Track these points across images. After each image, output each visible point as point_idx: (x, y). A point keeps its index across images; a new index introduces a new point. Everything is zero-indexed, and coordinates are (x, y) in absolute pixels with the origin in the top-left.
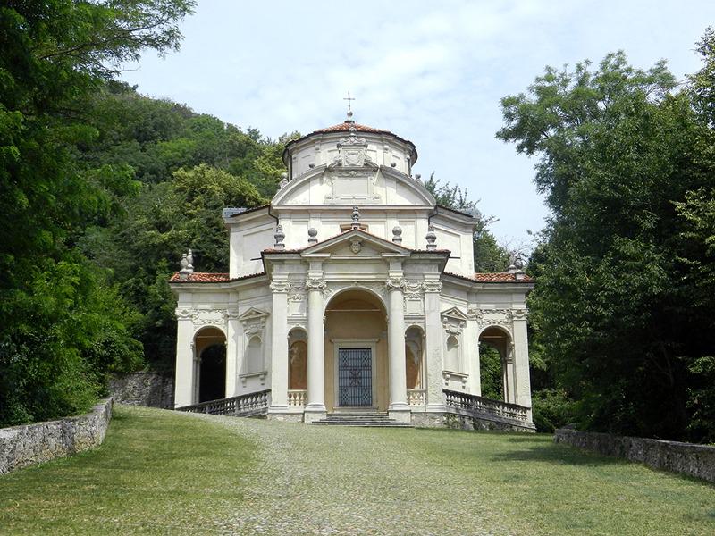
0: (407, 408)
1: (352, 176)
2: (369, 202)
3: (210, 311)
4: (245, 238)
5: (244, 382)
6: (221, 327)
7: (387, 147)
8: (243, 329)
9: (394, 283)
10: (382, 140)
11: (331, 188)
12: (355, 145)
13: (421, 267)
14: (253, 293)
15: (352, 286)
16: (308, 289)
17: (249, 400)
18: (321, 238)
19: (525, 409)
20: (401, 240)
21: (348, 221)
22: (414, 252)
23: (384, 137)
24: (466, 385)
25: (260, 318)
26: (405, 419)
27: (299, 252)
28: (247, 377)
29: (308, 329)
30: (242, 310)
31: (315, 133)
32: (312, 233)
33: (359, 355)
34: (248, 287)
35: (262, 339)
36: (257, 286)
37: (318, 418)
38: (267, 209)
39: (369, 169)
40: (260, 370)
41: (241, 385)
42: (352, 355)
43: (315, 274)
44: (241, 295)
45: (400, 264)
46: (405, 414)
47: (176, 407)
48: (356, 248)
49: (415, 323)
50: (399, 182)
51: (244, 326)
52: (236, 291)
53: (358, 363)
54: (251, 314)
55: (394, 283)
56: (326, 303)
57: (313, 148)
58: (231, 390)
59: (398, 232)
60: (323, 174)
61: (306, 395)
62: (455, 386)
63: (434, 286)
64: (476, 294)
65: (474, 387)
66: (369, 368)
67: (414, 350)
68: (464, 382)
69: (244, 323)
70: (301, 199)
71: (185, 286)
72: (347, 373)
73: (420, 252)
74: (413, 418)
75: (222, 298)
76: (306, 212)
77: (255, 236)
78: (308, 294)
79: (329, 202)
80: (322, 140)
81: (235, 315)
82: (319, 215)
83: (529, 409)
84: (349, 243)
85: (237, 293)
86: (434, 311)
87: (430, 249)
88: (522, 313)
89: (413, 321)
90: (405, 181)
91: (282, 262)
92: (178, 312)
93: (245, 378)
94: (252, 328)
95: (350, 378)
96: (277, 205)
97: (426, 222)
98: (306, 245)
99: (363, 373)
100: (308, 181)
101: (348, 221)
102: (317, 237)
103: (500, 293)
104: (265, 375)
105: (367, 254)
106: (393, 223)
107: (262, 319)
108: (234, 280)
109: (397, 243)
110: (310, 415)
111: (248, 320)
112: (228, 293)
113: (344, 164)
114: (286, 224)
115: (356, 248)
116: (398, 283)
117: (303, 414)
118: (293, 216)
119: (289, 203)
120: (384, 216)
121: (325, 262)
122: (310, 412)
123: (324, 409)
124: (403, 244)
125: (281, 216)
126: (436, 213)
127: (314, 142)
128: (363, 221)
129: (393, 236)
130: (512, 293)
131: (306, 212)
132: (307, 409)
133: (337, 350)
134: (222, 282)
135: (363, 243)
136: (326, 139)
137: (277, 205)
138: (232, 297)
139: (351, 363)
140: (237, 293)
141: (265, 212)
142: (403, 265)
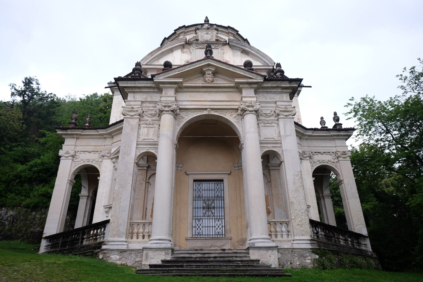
3: (90, 152)
8: (113, 165)
9: (248, 106)
10: (228, 33)
13: (272, 96)
15: (205, 113)
23: (230, 31)
31: (180, 28)
33: (212, 185)
42: (205, 186)
45: (252, 91)
46: (270, 252)
47: (44, 236)
48: (209, 77)
51: (114, 163)
53: (211, 194)
55: (248, 106)
56: (178, 129)
63: (288, 111)
64: (307, 139)
66: (222, 198)
69: (114, 160)
71: (69, 132)
72: (201, 204)
75: (100, 142)
80: (185, 33)
86: (290, 135)
88: (346, 154)
89: (268, 145)
92: (61, 153)
95: (203, 208)
96: (146, 65)
103: (325, 139)
105: (220, 82)
110: (151, 253)
113: (200, 39)
115: (209, 77)
116: (252, 106)
122: (151, 249)
123: (169, 245)
130: (334, 139)
135: (216, 73)
136: (188, 32)
137: (146, 65)
138: (108, 142)
139: (205, 194)
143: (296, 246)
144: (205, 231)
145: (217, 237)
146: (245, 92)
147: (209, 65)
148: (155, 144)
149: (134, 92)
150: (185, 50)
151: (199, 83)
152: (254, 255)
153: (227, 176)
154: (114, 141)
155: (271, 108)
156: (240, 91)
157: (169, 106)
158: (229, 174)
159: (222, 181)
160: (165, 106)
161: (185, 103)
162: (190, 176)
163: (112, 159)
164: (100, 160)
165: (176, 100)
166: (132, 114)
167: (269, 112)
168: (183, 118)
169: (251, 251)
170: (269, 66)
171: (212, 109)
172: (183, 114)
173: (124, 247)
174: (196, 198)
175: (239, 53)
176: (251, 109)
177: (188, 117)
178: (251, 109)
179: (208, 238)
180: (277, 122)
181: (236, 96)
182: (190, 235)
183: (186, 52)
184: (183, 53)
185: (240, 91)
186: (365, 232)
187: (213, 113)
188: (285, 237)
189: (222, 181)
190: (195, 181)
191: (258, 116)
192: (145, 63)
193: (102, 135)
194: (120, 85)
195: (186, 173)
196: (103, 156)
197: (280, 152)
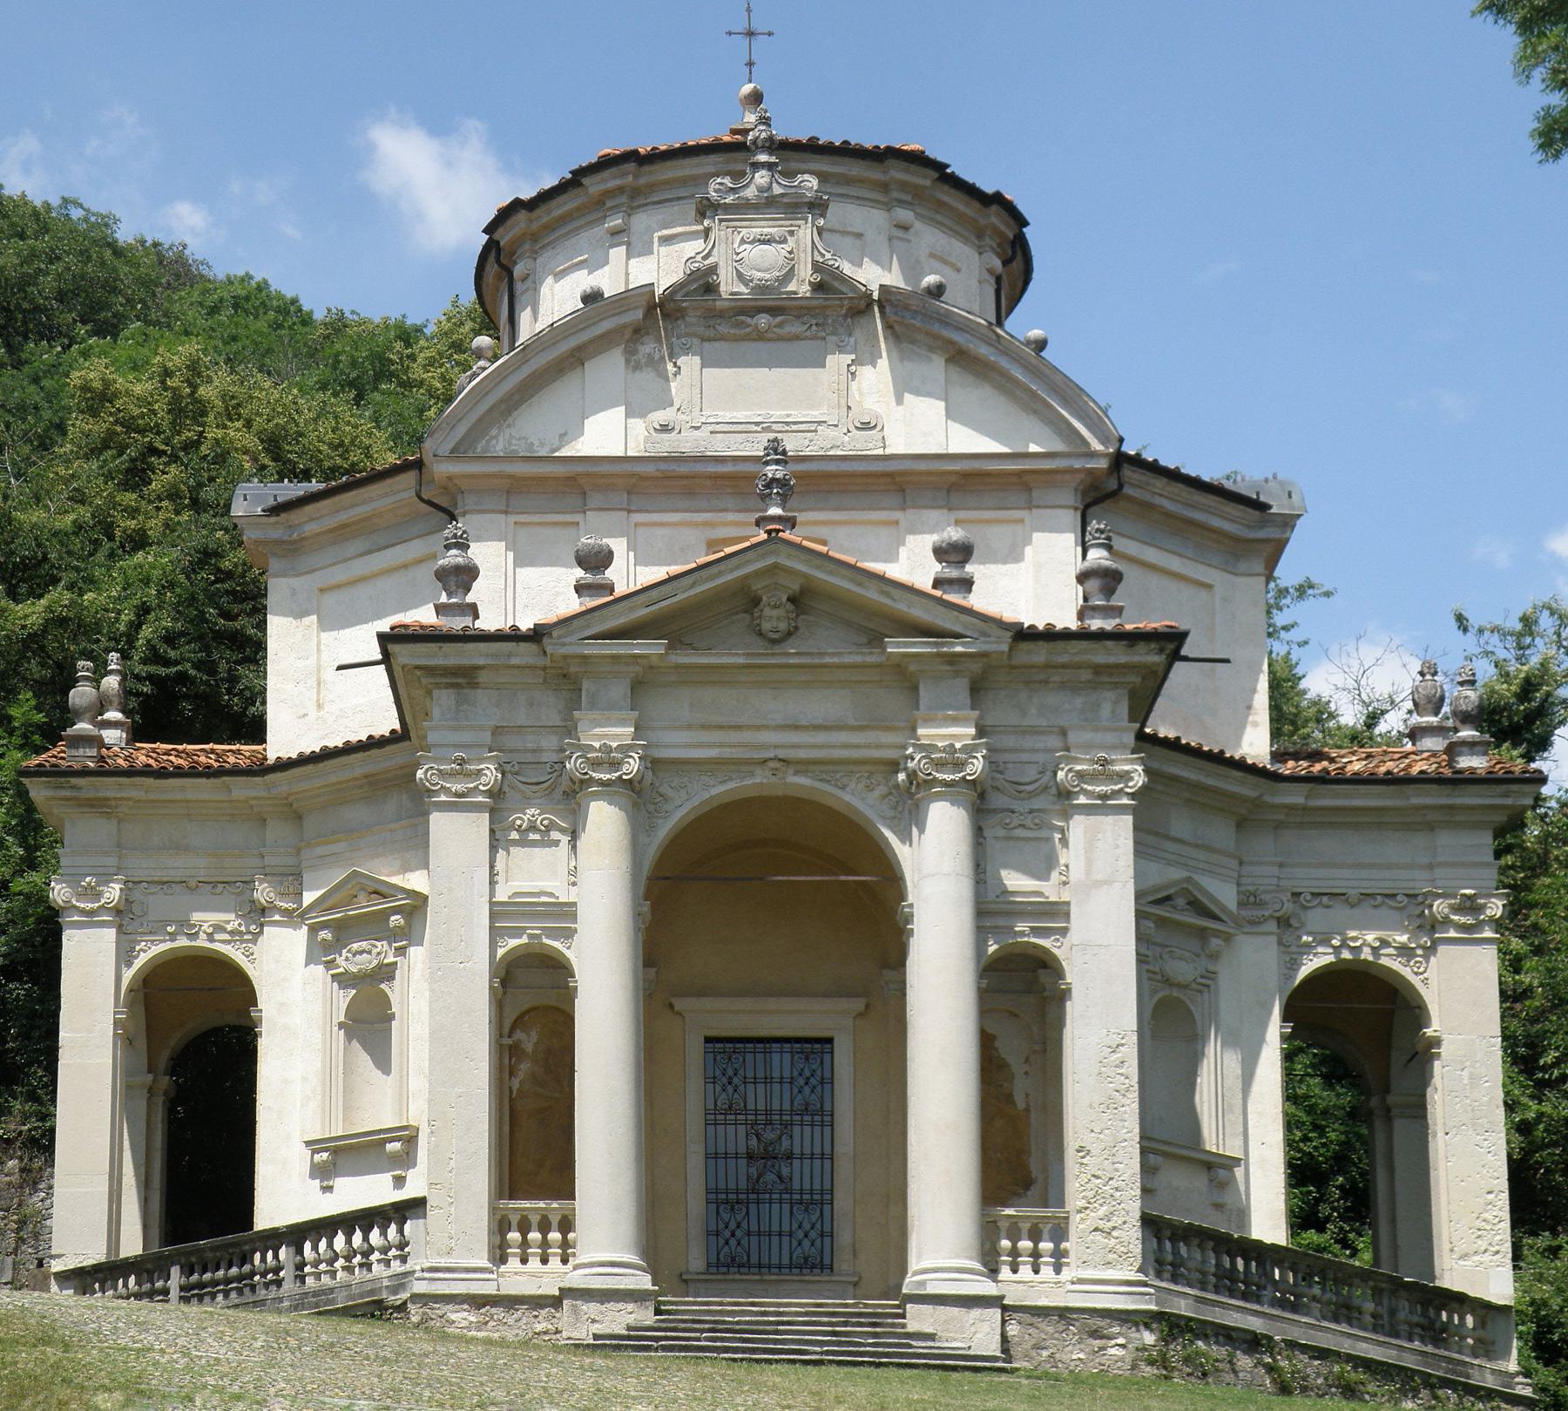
6: (235, 954)
7: (904, 214)
13: (1052, 699)
17: (339, 1241)
27: (538, 634)
28: (335, 1152)
102: (611, 574)
108: (283, 765)
113: (728, 285)
129: (935, 568)
142: (977, 690)
147: (776, 567)
167: (1031, 773)
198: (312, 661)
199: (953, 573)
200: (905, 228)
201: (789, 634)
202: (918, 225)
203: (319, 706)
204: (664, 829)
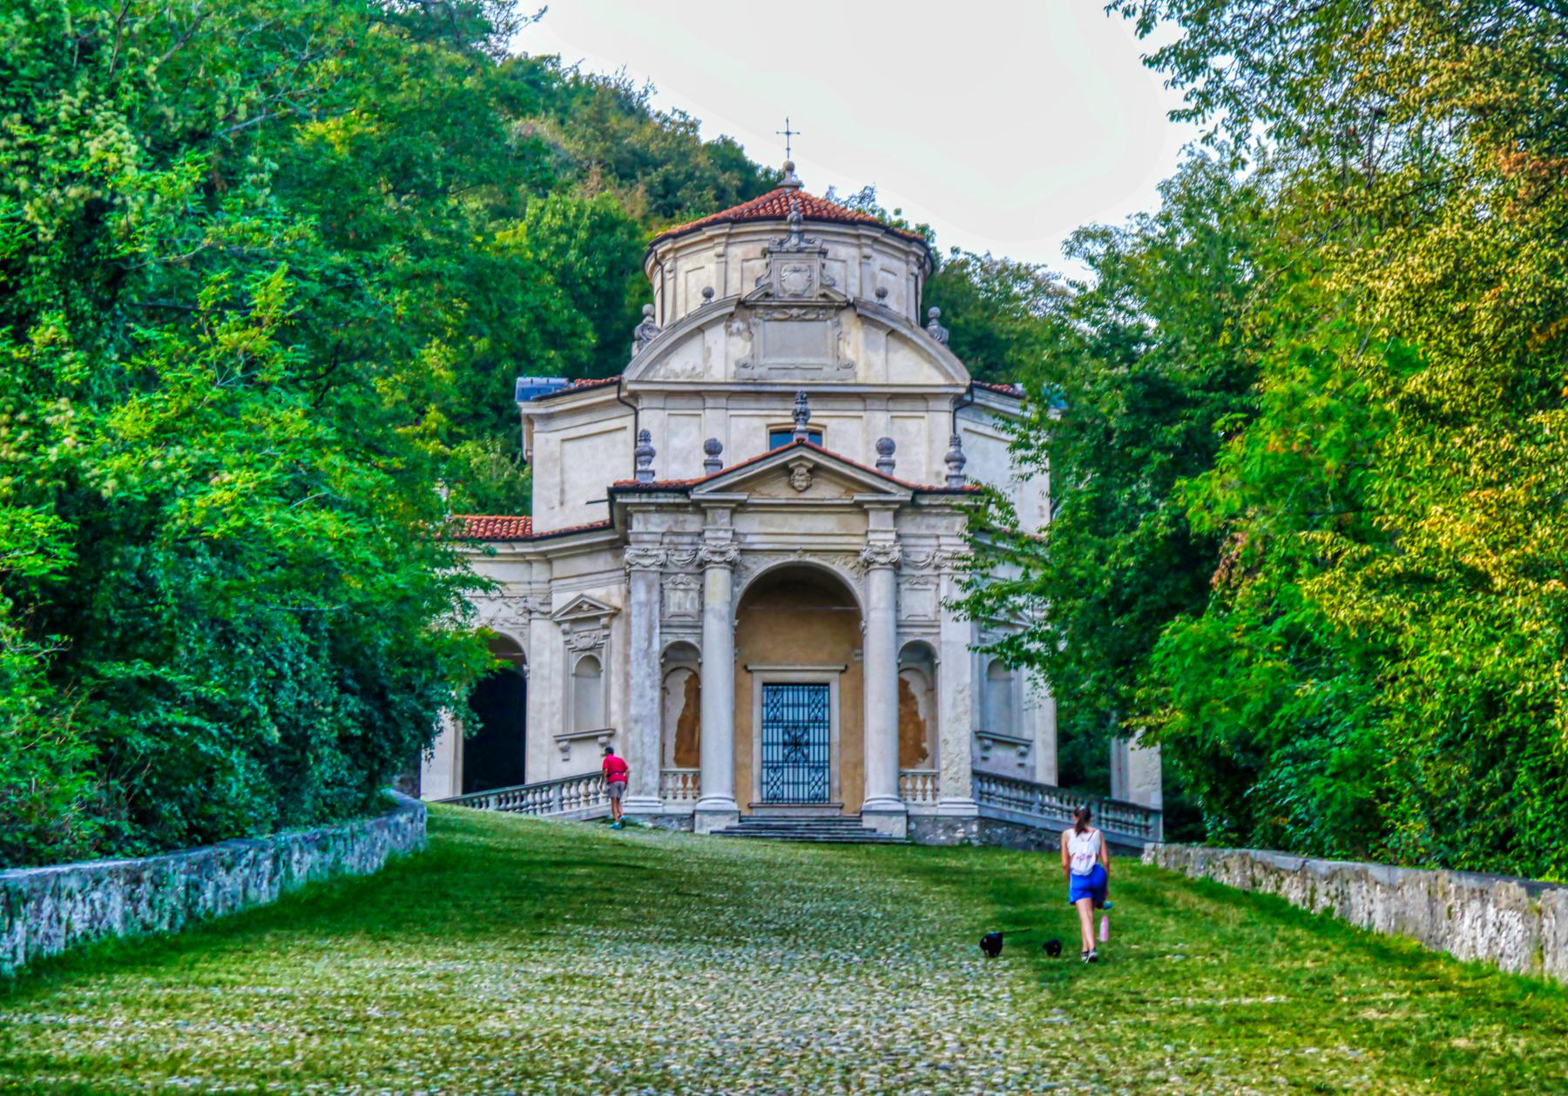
0: (901, 807)
1: (790, 319)
2: (828, 375)
4: (568, 445)
5: (564, 750)
6: (515, 636)
7: (867, 251)
8: (561, 639)
10: (858, 237)
11: (749, 345)
12: (800, 251)
13: (932, 521)
14: (583, 564)
15: (792, 558)
16: (702, 565)
17: (582, 789)
18: (728, 460)
19: (1148, 812)
20: (892, 464)
21: (782, 415)
22: (918, 492)
24: (1028, 761)
25: (597, 618)
26: (896, 828)
27: (683, 489)
28: (572, 740)
29: (701, 642)
30: (561, 600)
32: (713, 448)
33: (804, 697)
34: (574, 553)
35: (603, 666)
36: (592, 550)
37: (722, 824)
38: (615, 388)
39: (830, 306)
40: (598, 724)
41: (559, 756)
42: (788, 696)
43: (719, 533)
44: (560, 568)
45: (890, 514)
46: (894, 819)
48: (800, 482)
49: (915, 635)
50: (892, 332)
51: (565, 633)
52: (547, 559)
53: (803, 714)
54: (579, 607)
55: (878, 554)
57: (711, 253)
58: (541, 762)
59: (886, 448)
60: (731, 315)
61: (697, 777)
62: (1003, 761)
65: (1043, 766)
66: (823, 723)
67: (916, 688)
68: (1023, 755)
69: (566, 626)
70: (684, 365)
72: (778, 735)
73: (931, 492)
74: (913, 826)
76: (698, 394)
77: (585, 443)
78: (702, 574)
79: (746, 373)
80: (729, 235)
81: (545, 609)
82: (722, 402)
83: (1155, 812)
84: (786, 470)
85: (550, 562)
87: (955, 484)
89: (915, 630)
90: (905, 331)
91: (643, 508)
93: (569, 741)
94: (585, 637)
95: (785, 744)
96: (637, 382)
97: (944, 419)
98: (696, 472)
99: (815, 735)
100: (700, 330)
101: (782, 415)
102: (721, 457)
104: (611, 735)
105: (825, 492)
106: (880, 422)
107: (604, 621)
108: (544, 538)
109: (885, 470)
110: (707, 819)
111: (575, 622)
112: (530, 562)
114: (650, 419)
117: (693, 816)
118: (671, 403)
119: (660, 373)
120: (859, 405)
121: (740, 508)
123: (734, 806)
124: (898, 475)
125: (643, 403)
126: (968, 398)
127: (711, 238)
128: (819, 415)
129: (878, 457)
131: (698, 394)
132: (700, 806)
133: (757, 688)
134: (518, 540)
135: (816, 470)
137: (637, 382)
138: (539, 572)
139: (789, 714)
140: (550, 562)
141: (610, 395)
142: (897, 515)
143: (941, 812)
144: (788, 792)
145: (817, 800)
146: (873, 518)
147: (801, 458)
148: (698, 626)
149: (644, 512)
150: (737, 325)
151: (780, 492)
152: (869, 822)
153: (836, 675)
154: (556, 574)
155: (927, 549)
156: (866, 513)
157: (722, 553)
158: (842, 672)
159: (827, 684)
160: (713, 553)
161: (749, 539)
162: (756, 675)
163: (559, 623)
164: (522, 620)
165: (734, 533)
166: (647, 562)
167: (922, 557)
168: (747, 568)
169: (865, 818)
170: (957, 386)
171: (806, 551)
172: (749, 560)
173: (659, 811)
174: (770, 723)
175: (882, 335)
176: (882, 559)
177: (758, 567)
178: (882, 559)
179: (796, 802)
180: (936, 580)
181: (856, 522)
182: (756, 799)
183: (739, 332)
184: (731, 334)
185: (866, 513)
186: (1155, 801)
187: (809, 559)
188: (929, 798)
189: (827, 684)
190: (765, 684)
191: (897, 575)
192: (634, 377)
193: (522, 555)
194: (619, 500)
195: (745, 667)
196: (530, 612)
197: (935, 645)
198: (557, 479)
199: (885, 459)
200: (868, 257)
201: (807, 488)
202: (874, 255)
203: (562, 504)
204: (746, 582)
